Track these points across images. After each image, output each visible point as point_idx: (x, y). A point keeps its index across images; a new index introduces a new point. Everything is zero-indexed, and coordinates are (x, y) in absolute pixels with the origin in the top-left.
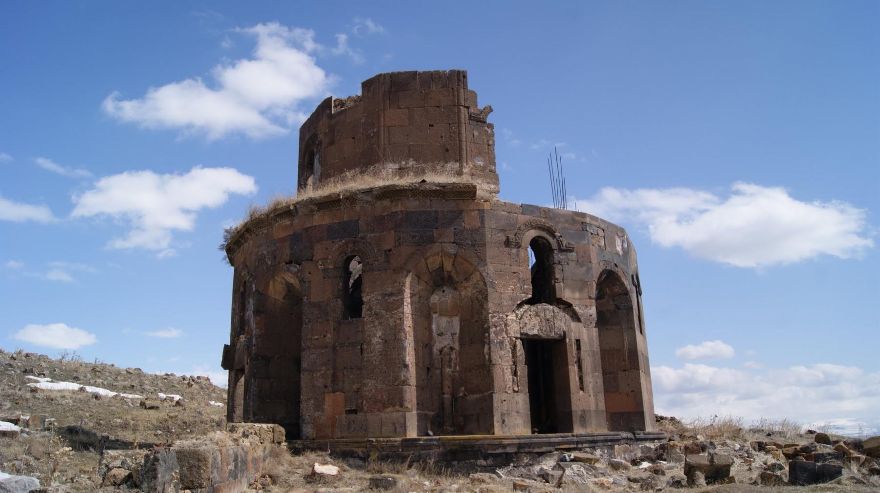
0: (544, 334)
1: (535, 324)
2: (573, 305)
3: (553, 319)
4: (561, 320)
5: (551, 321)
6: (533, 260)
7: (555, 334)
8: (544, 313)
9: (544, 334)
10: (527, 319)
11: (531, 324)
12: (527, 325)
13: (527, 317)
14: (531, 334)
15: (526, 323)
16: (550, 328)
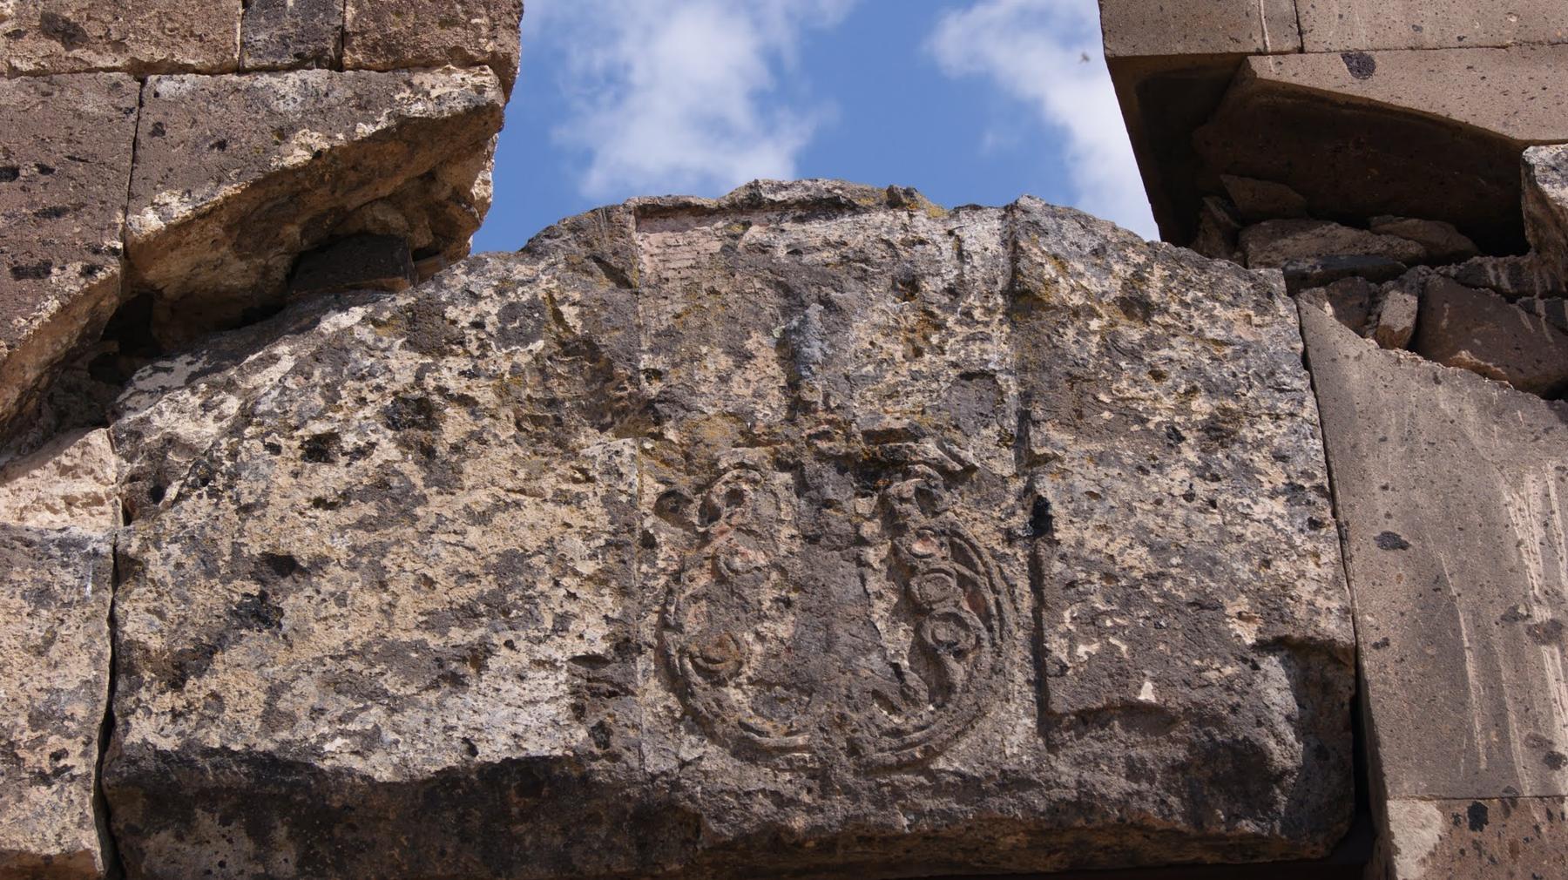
0: (748, 749)
1: (511, 564)
2: (1537, 156)
3: (1018, 441)
4: (1217, 432)
5: (959, 476)
6: (1415, 221)
7: (1047, 721)
8: (790, 354)
9: (748, 749)
10: (330, 477)
11: (402, 563)
12: (294, 603)
13: (319, 450)
14: (381, 768)
15: (282, 565)
16: (913, 610)
